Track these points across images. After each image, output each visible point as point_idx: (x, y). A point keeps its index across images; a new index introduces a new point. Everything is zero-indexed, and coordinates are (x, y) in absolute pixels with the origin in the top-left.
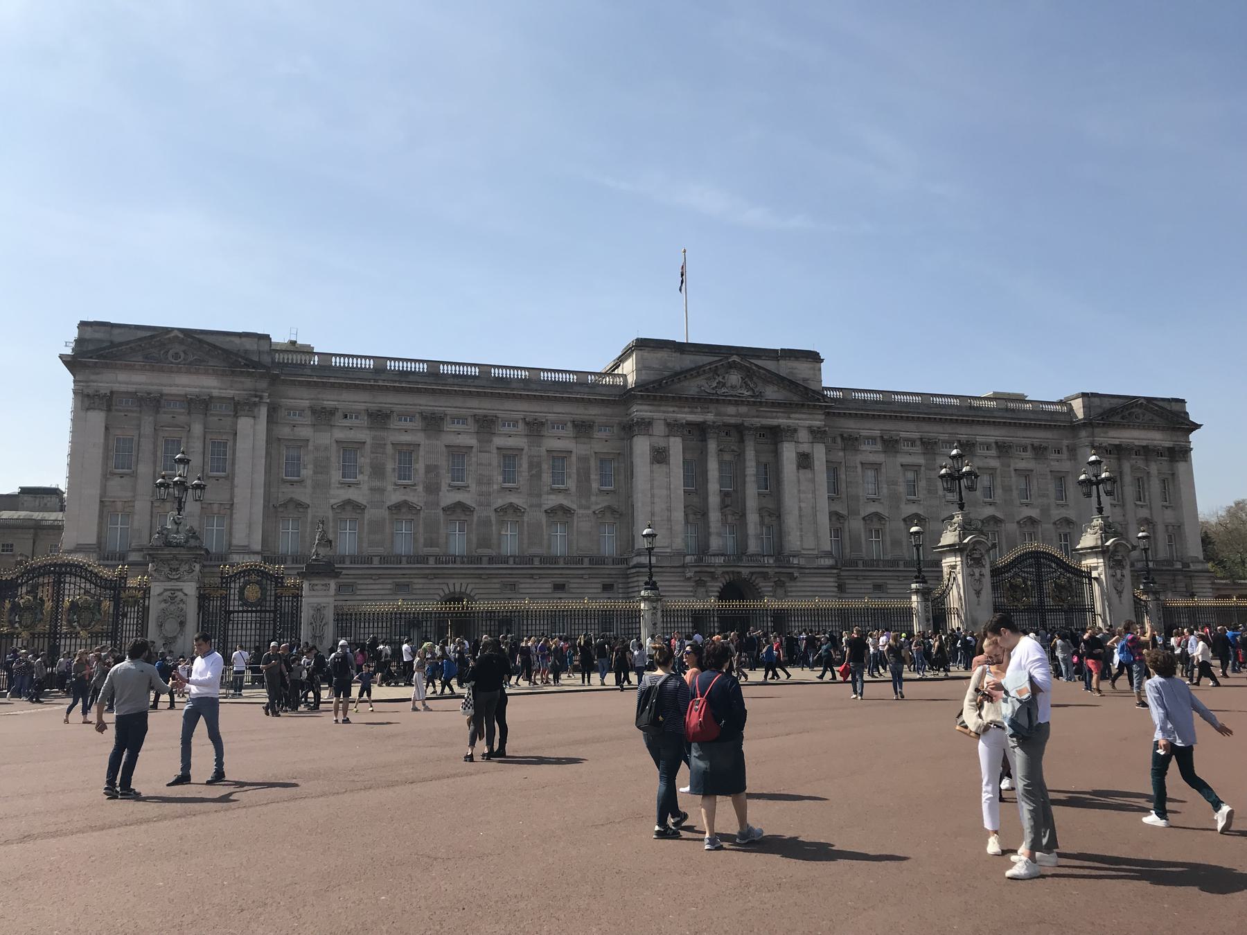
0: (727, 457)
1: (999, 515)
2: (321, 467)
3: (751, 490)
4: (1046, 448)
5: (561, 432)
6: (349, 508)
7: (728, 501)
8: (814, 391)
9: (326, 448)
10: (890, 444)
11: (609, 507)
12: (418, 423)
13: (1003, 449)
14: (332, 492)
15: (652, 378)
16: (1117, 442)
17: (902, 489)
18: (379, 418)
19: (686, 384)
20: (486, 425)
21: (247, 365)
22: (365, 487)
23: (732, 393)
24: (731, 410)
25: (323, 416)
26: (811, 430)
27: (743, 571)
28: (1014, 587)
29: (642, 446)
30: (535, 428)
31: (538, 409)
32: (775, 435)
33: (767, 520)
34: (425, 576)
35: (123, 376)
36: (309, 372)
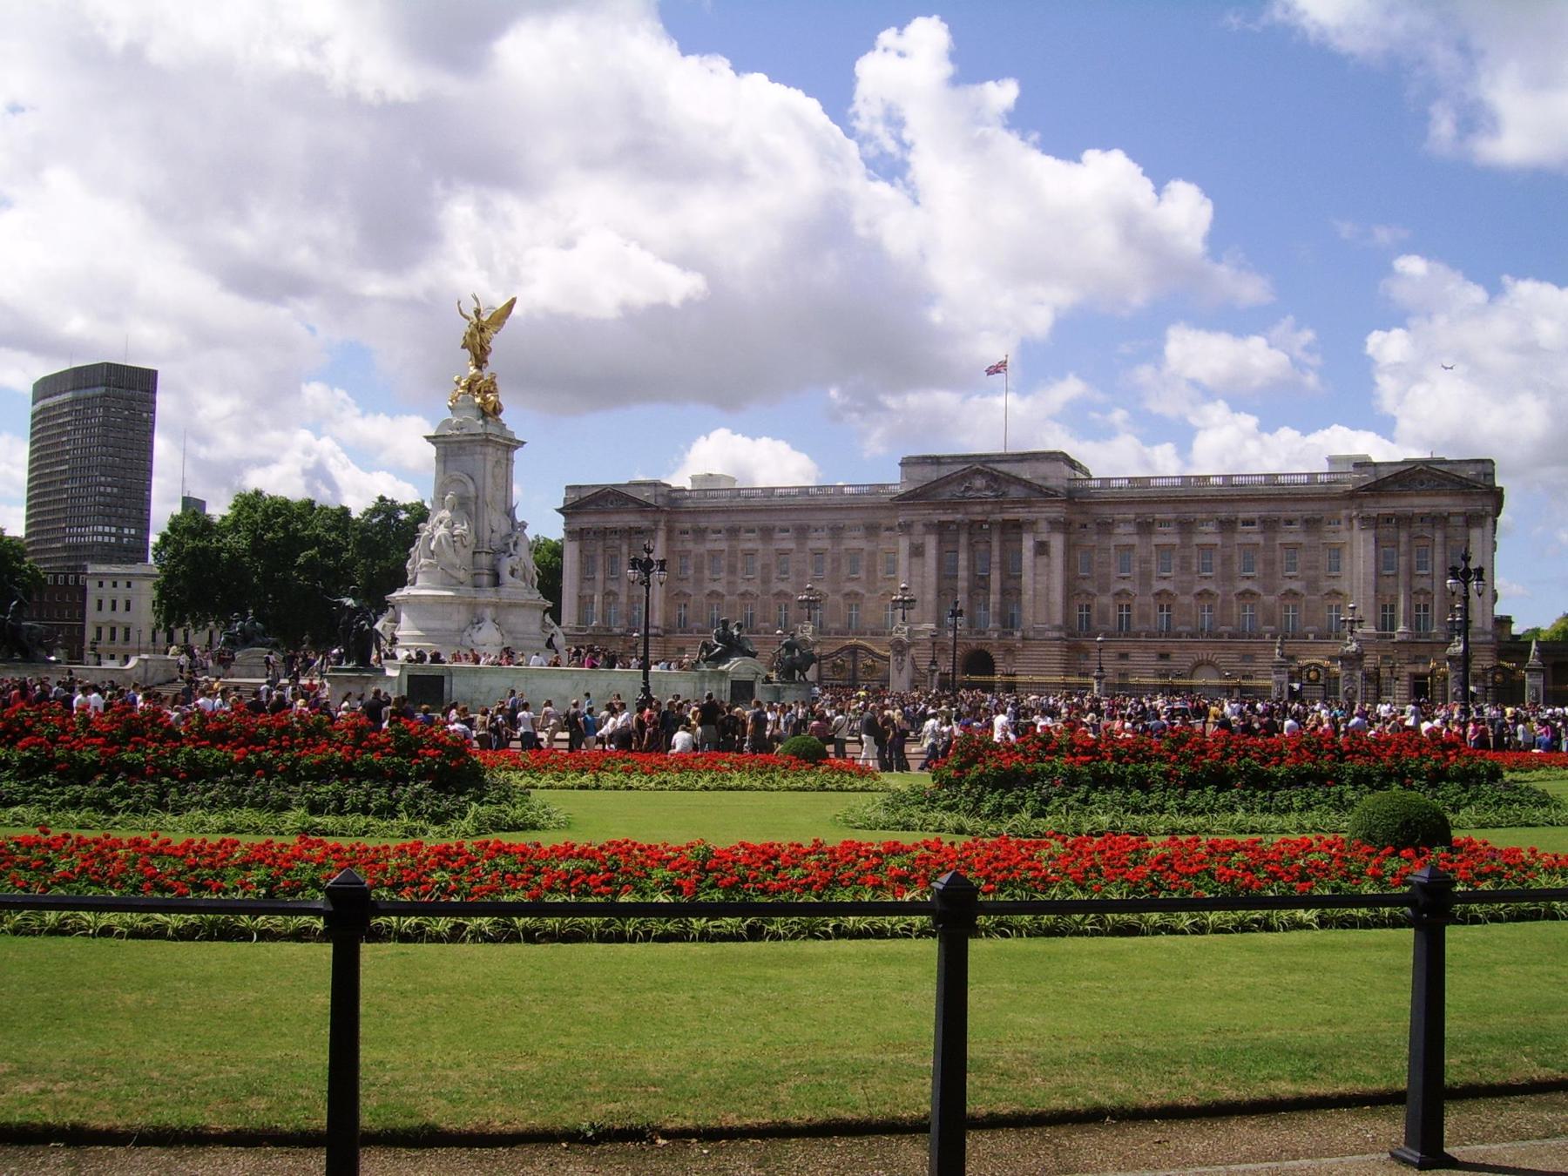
0: (982, 547)
1: (1255, 589)
2: (699, 569)
3: (995, 576)
4: (1320, 521)
5: (856, 534)
9: (702, 555)
10: (1145, 527)
13: (1269, 525)
16: (1391, 511)
17: (1154, 567)
18: (733, 532)
22: (724, 582)
24: (978, 509)
30: (836, 532)
32: (1017, 526)
35: (585, 519)
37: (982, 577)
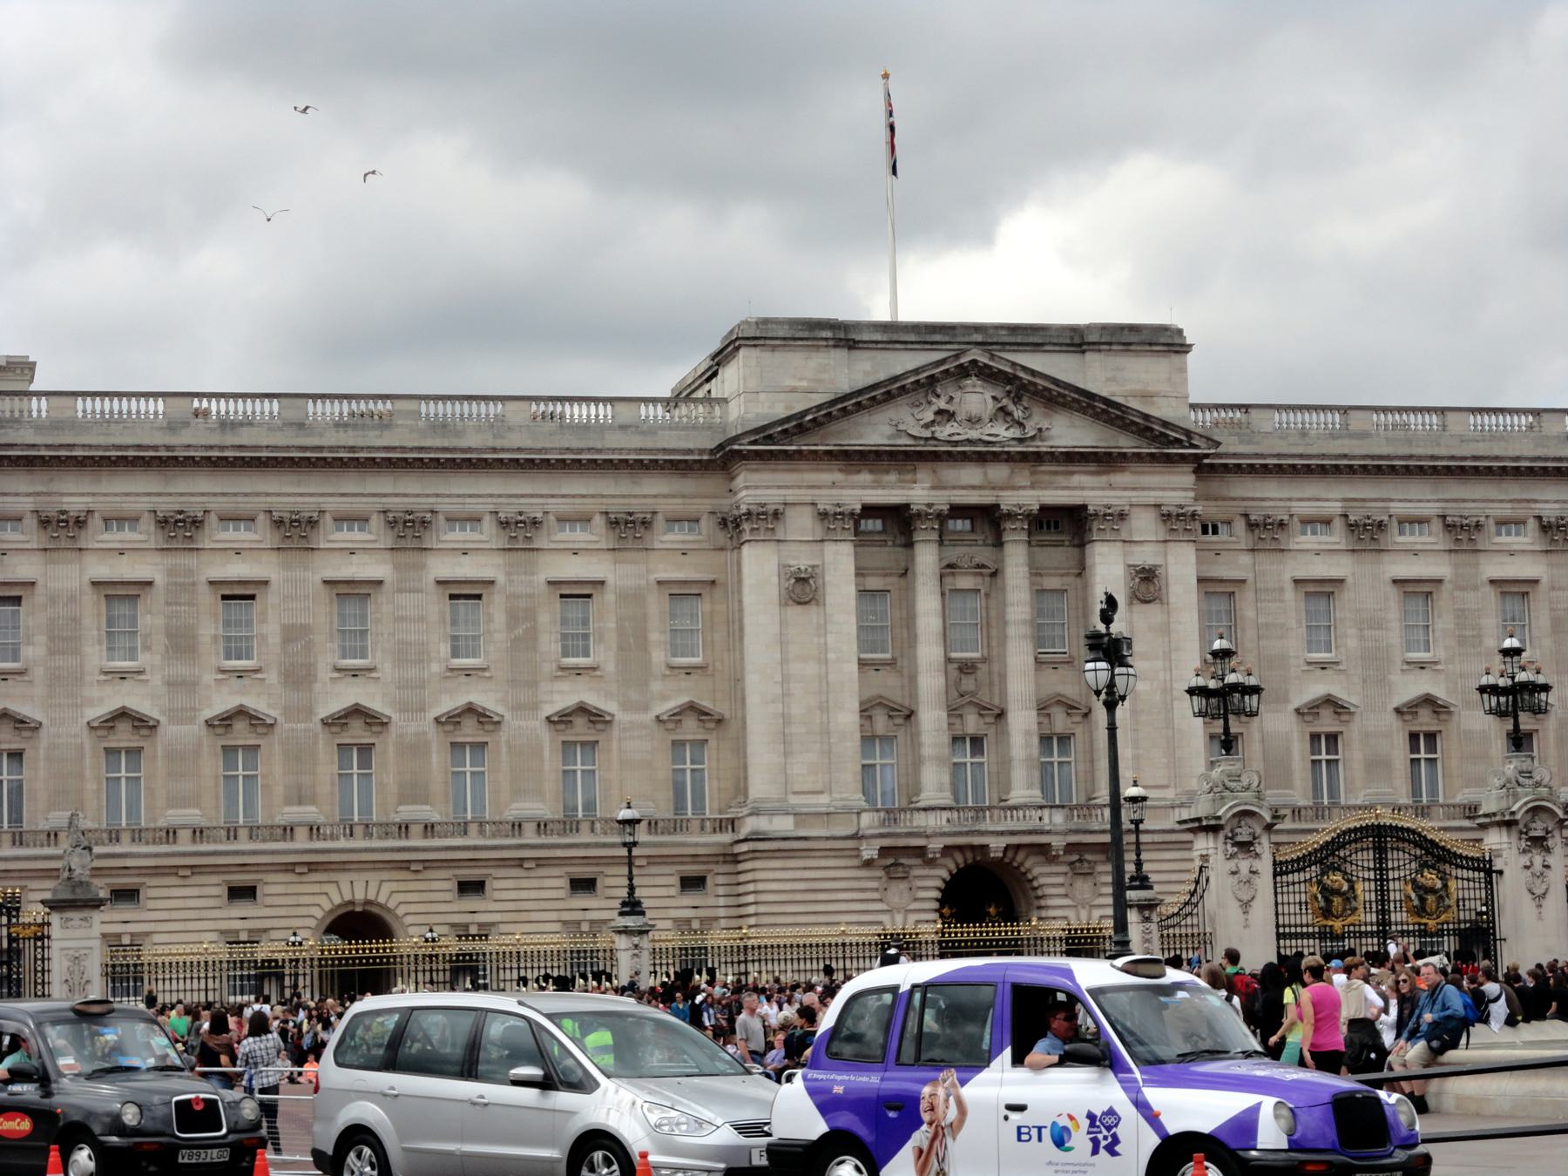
0: (965, 582)
2: (64, 640)
3: (1019, 657)
5: (578, 536)
6: (123, 727)
7: (968, 684)
8: (1165, 424)
9: (72, 599)
10: (1367, 533)
11: (692, 708)
12: (260, 534)
14: (87, 692)
15: (781, 411)
17: (1394, 636)
18: (180, 528)
19: (863, 417)
20: (410, 529)
22: (156, 679)
23: (974, 434)
24: (970, 474)
25: (63, 528)
27: (996, 844)
28: (1328, 892)
29: (760, 567)
30: (520, 531)
31: (530, 491)
33: (1060, 722)
34: (289, 868)
36: (27, 436)
37: (967, 668)
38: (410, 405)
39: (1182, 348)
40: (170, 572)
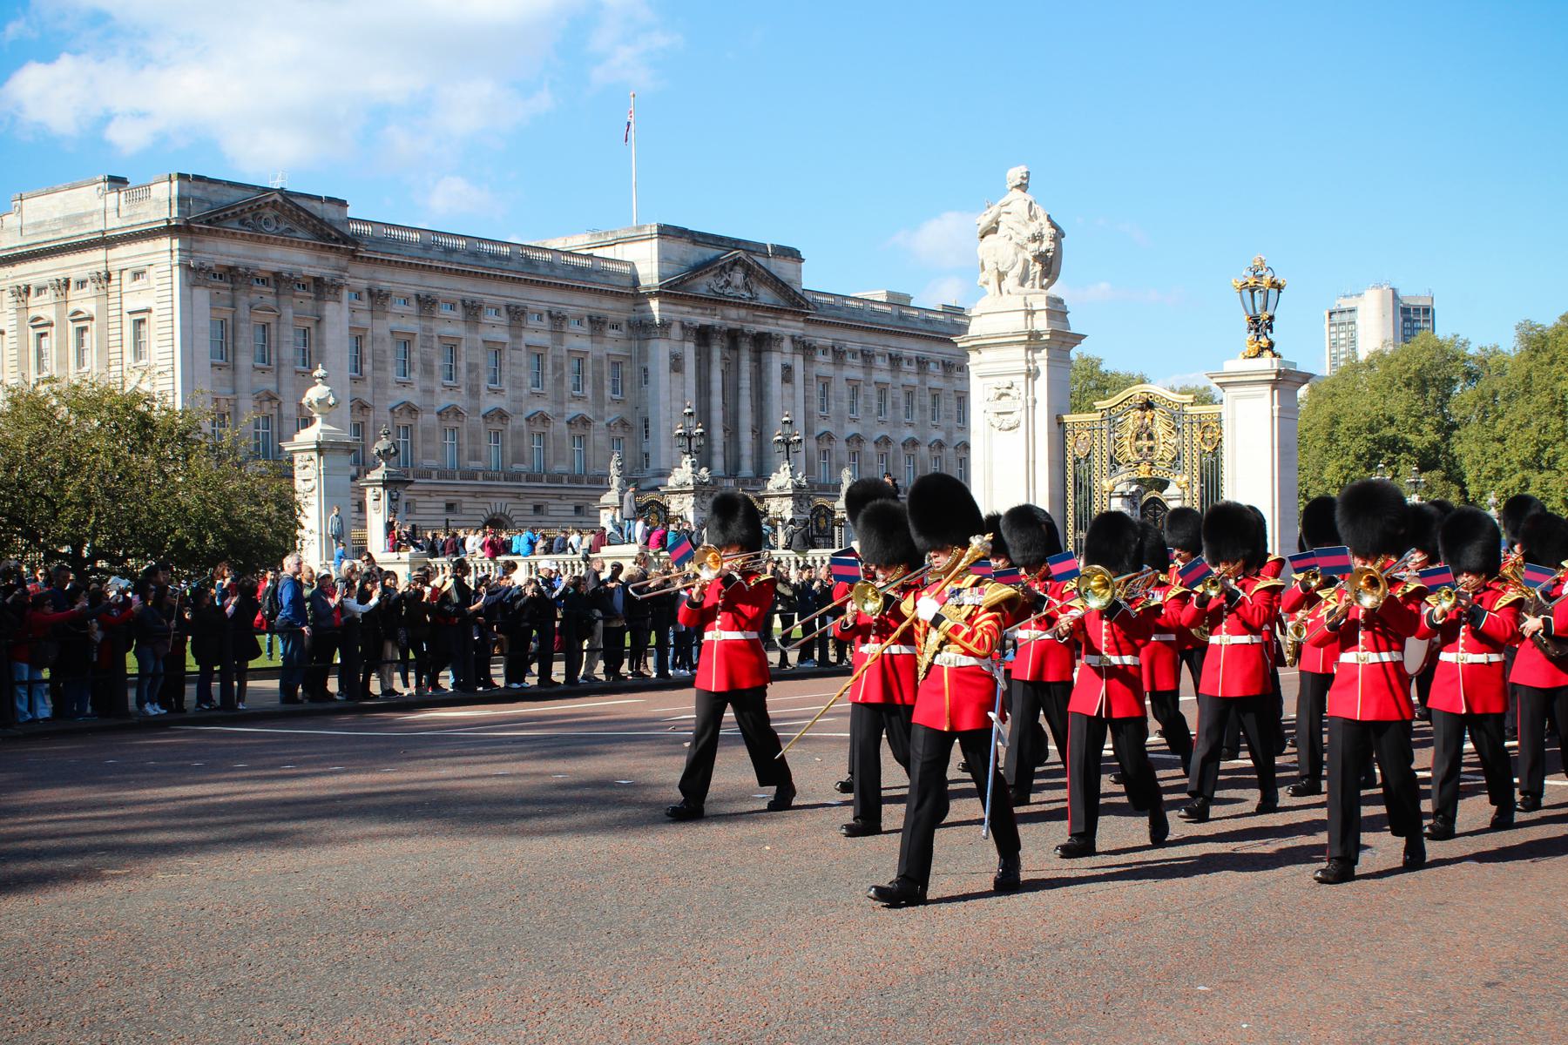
2: (379, 364)
3: (746, 405)
5: (579, 329)
10: (838, 354)
13: (922, 363)
14: (390, 392)
17: (846, 406)
20: (516, 314)
21: (337, 240)
22: (417, 387)
23: (738, 294)
24: (733, 313)
26: (793, 338)
29: (660, 351)
30: (557, 320)
31: (560, 300)
38: (515, 249)
39: (801, 260)
40: (424, 329)
